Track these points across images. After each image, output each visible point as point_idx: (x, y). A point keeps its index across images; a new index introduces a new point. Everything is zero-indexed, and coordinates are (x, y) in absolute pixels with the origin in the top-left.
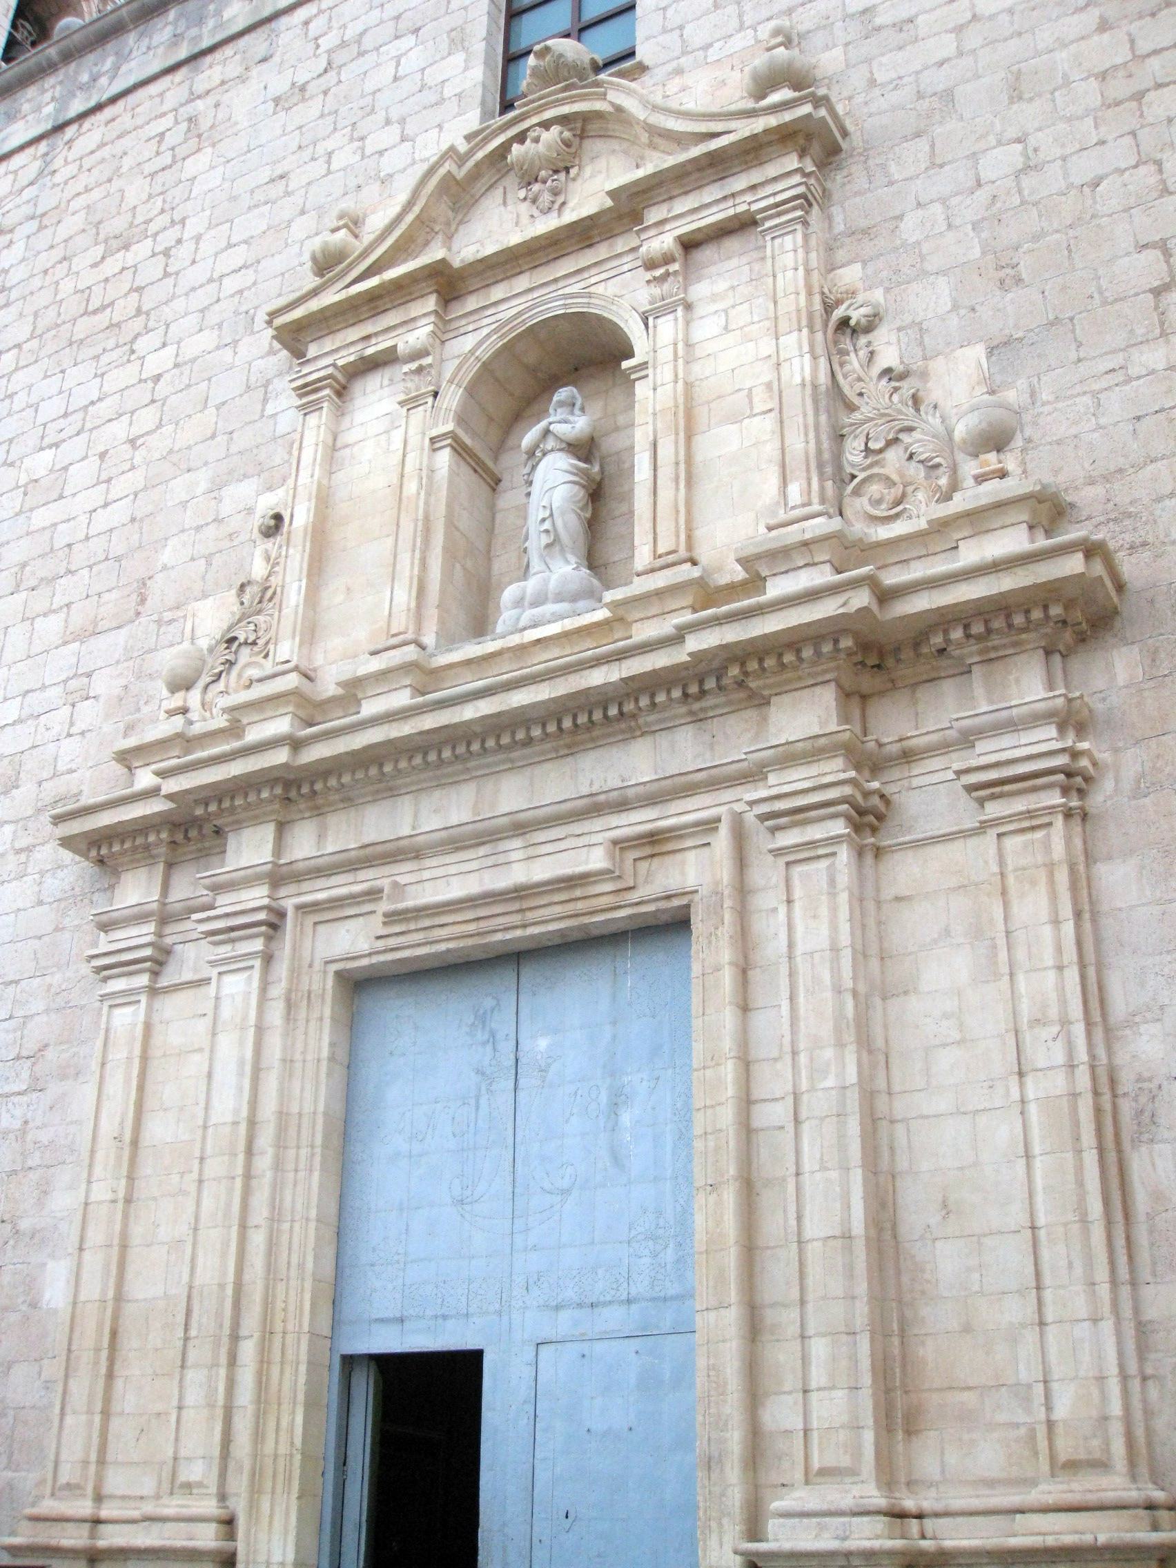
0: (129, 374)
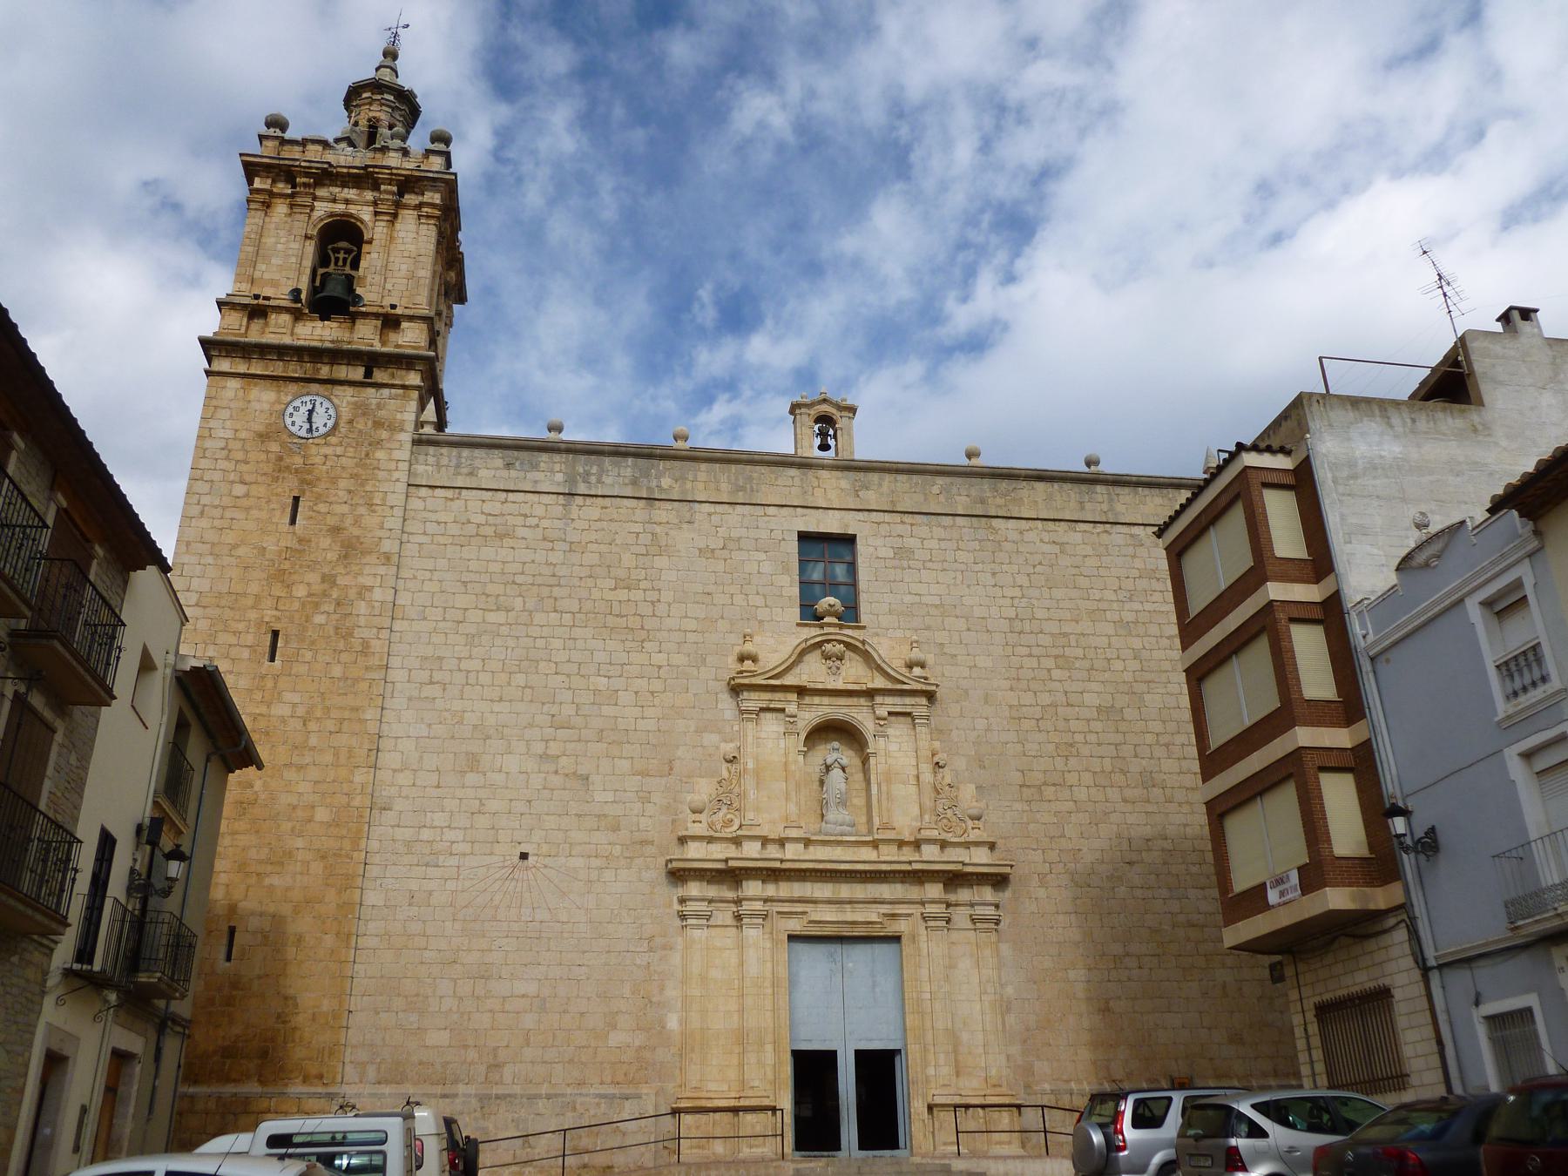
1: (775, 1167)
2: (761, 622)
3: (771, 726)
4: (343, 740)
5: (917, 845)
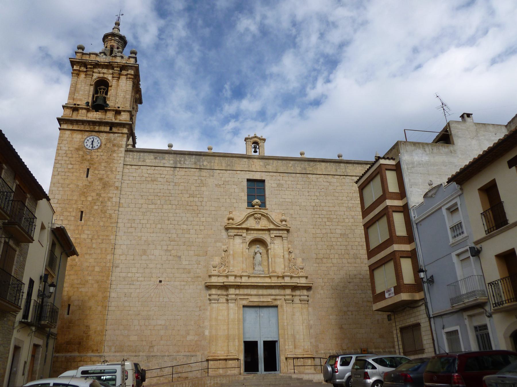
0: (197, 219)
1: (238, 377)
2: (235, 207)
3: (238, 240)
4: (103, 246)
5: (283, 277)
